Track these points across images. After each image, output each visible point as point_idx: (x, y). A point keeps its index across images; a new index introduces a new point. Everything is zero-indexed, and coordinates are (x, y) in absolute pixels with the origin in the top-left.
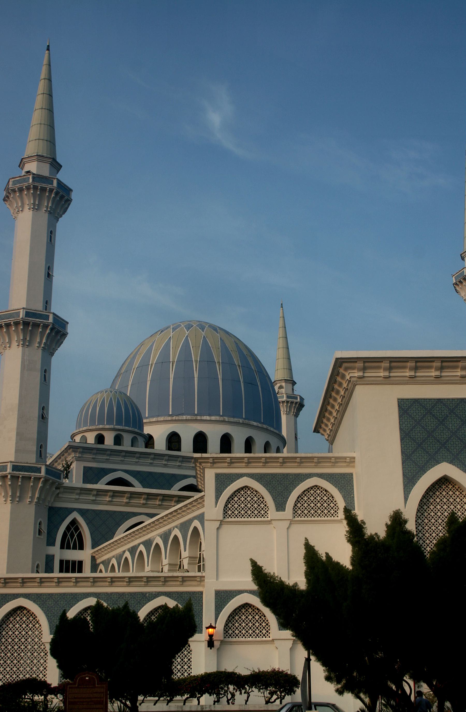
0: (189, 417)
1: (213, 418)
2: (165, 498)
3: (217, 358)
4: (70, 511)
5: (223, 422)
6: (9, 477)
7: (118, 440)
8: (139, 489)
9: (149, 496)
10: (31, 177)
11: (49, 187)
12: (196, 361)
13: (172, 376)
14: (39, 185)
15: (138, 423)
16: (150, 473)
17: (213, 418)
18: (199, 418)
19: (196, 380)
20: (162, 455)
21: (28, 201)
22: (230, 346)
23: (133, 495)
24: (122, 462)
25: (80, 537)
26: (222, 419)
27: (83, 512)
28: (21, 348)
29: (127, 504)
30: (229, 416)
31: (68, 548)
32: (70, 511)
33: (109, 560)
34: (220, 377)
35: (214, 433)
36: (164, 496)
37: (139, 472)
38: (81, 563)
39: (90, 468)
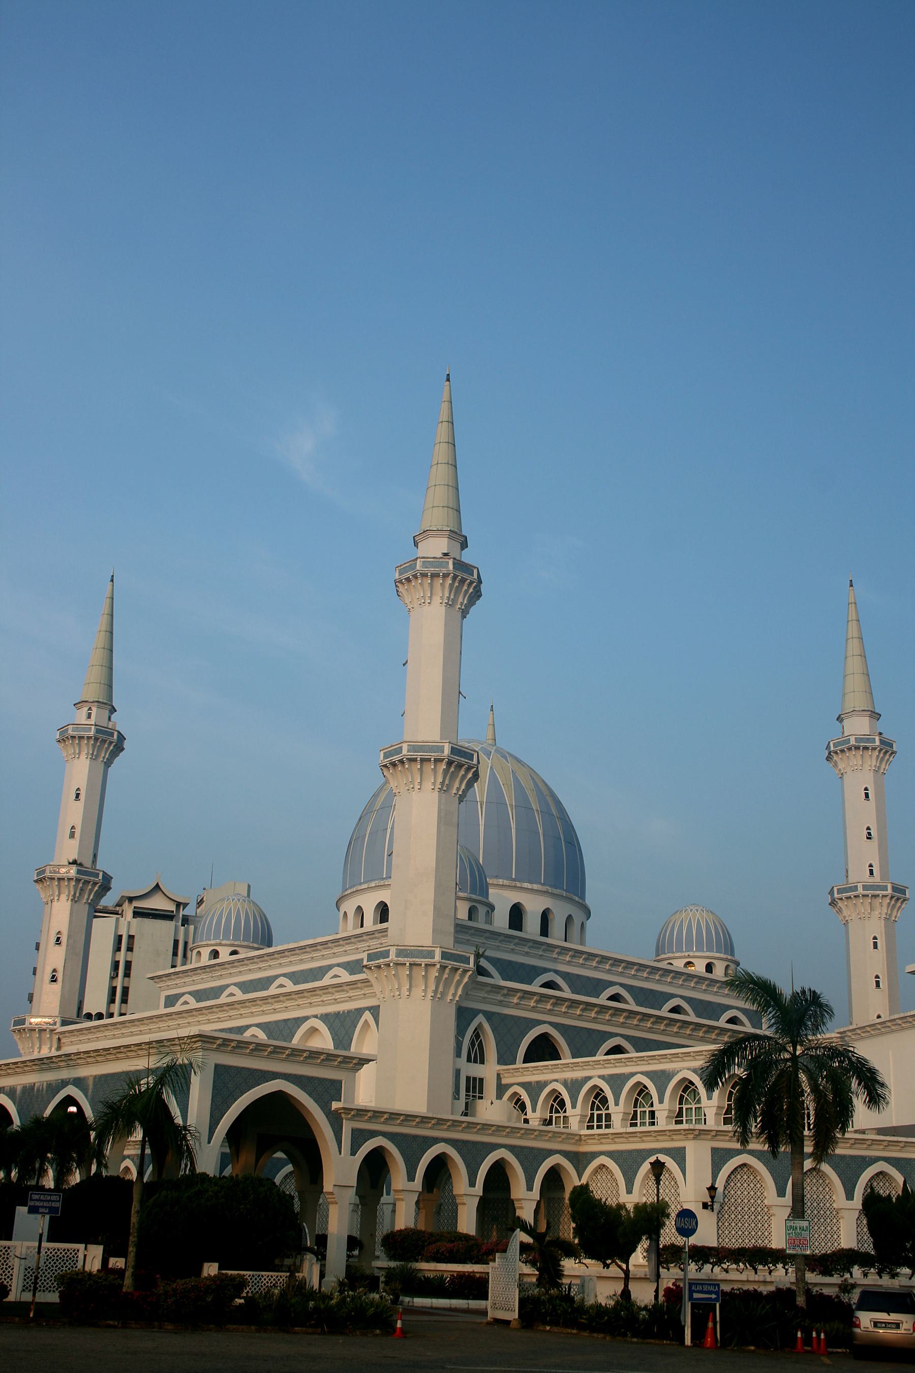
0: (506, 882)
1: (535, 887)
2: (589, 1006)
3: (535, 806)
4: (475, 1013)
5: (546, 892)
6: (438, 966)
7: (472, 913)
8: (567, 994)
9: (574, 1003)
10: (451, 562)
11: (469, 579)
12: (511, 805)
13: (482, 822)
14: (461, 575)
15: (484, 891)
17: (535, 887)
18: (518, 884)
19: (513, 831)
20: (500, 934)
21: (442, 590)
22: (528, 785)
23: (560, 1001)
26: (544, 888)
27: (489, 1016)
28: (436, 793)
29: (534, 1009)
30: (551, 886)
32: (475, 1013)
33: (542, 1085)
34: (541, 831)
35: (534, 906)
36: (526, 992)
37: (499, 960)
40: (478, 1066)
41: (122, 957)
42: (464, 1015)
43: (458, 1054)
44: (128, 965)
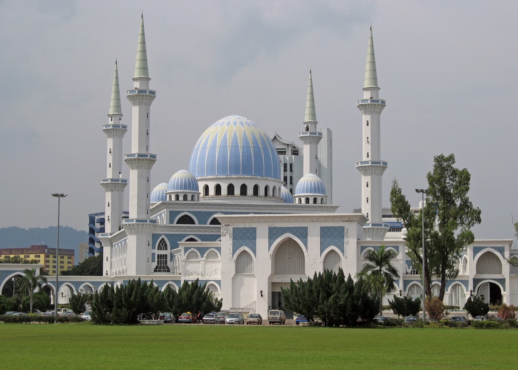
4: (160, 235)
16: (200, 212)
24: (187, 208)
25: (166, 245)
27: (165, 235)
31: (161, 249)
32: (160, 235)
37: (194, 212)
38: (166, 255)
40: (165, 251)
41: (288, 174)
42: (155, 237)
43: (154, 248)
44: (291, 178)
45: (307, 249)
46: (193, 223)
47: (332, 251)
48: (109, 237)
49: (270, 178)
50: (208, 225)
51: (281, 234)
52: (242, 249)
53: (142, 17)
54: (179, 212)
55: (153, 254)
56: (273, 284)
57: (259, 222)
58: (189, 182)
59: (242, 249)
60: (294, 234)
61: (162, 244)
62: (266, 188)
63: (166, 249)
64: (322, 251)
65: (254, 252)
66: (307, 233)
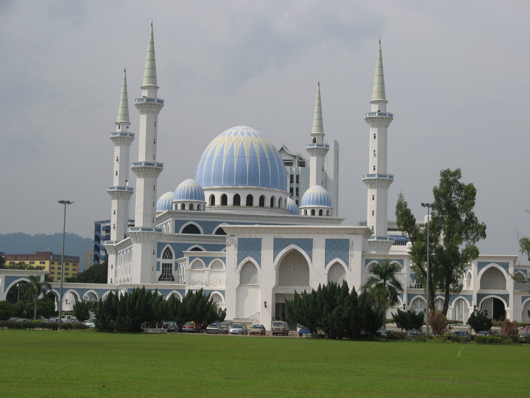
4: (166, 244)
16: (205, 222)
24: (192, 217)
25: (171, 254)
27: (171, 244)
31: (166, 258)
32: (166, 244)
37: (200, 221)
38: (171, 264)
39: (178, 220)
41: (295, 185)
42: (160, 245)
43: (159, 257)
44: (297, 189)
45: (311, 261)
46: (199, 232)
47: (337, 263)
48: (115, 245)
49: (276, 189)
50: (213, 235)
51: (286, 246)
52: (247, 259)
53: (152, 26)
54: (185, 222)
55: (158, 263)
56: (277, 296)
57: (264, 233)
58: (195, 191)
59: (247, 259)
60: (299, 246)
61: (167, 253)
62: (272, 199)
63: (171, 258)
64: (326, 263)
65: (259, 262)
66: (312, 245)
